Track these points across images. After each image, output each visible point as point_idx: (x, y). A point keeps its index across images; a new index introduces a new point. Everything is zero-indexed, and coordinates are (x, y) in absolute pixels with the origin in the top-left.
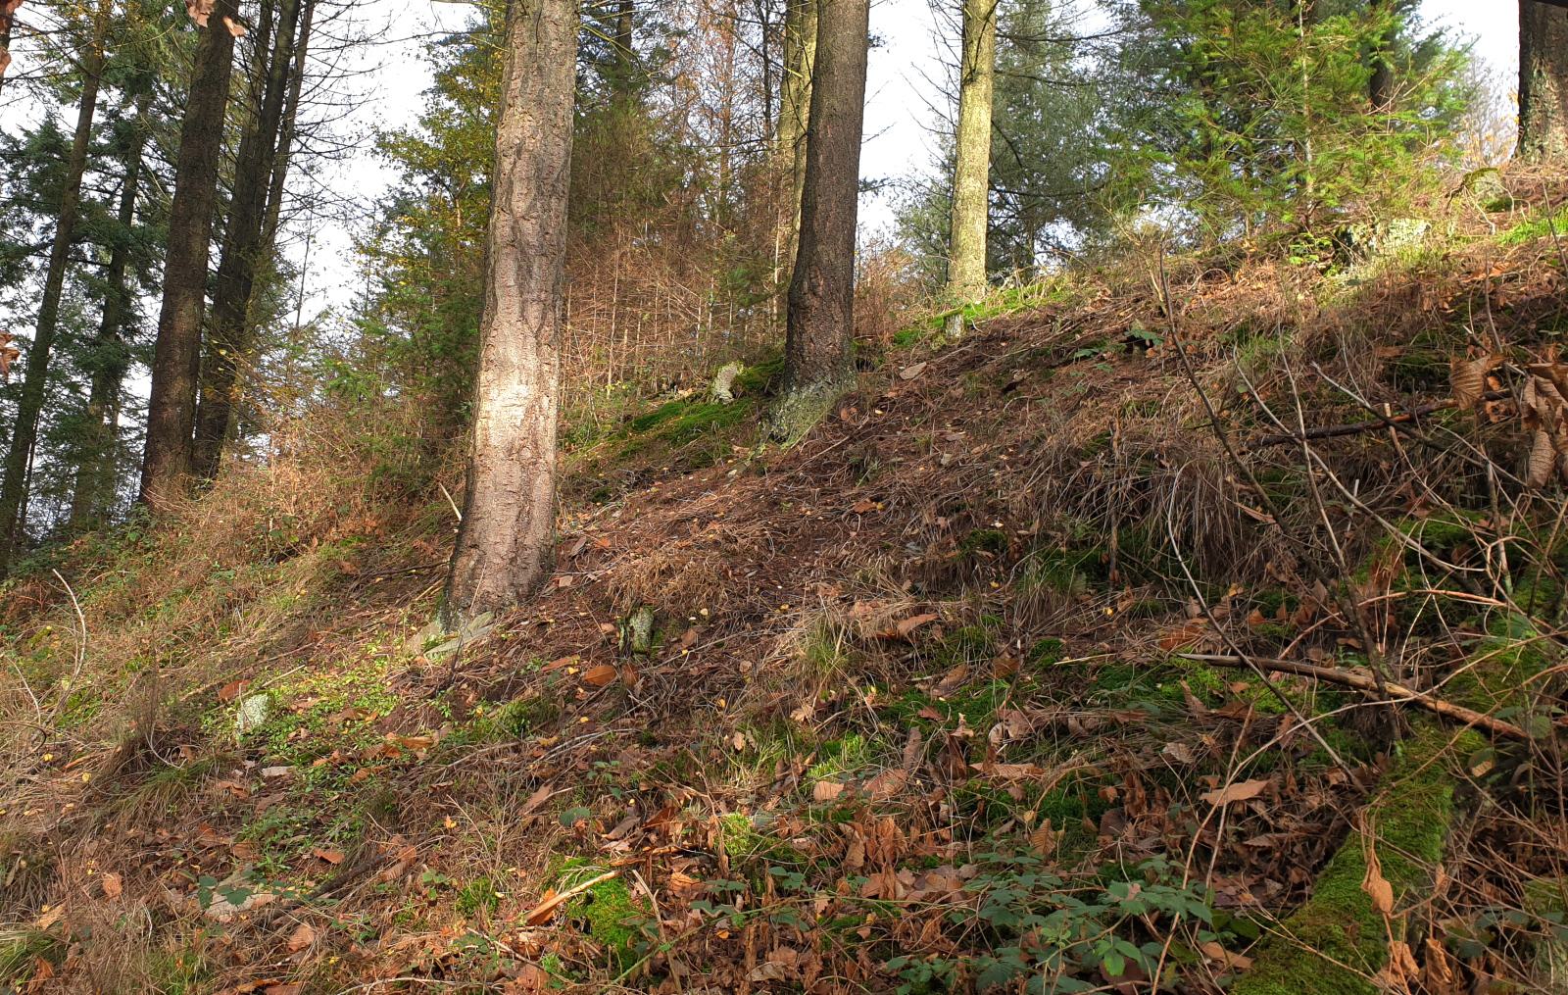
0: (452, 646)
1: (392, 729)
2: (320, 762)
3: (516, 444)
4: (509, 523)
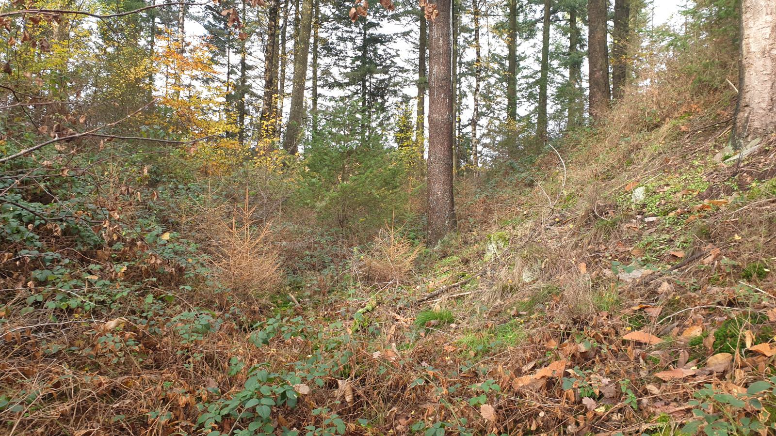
0: (737, 157)
1: (707, 198)
2: (672, 214)
3: (768, 48)
4: (766, 91)
